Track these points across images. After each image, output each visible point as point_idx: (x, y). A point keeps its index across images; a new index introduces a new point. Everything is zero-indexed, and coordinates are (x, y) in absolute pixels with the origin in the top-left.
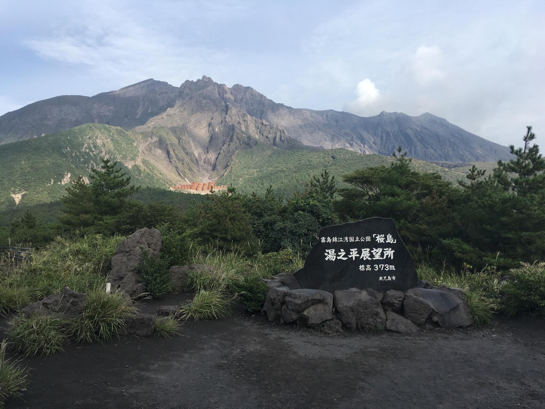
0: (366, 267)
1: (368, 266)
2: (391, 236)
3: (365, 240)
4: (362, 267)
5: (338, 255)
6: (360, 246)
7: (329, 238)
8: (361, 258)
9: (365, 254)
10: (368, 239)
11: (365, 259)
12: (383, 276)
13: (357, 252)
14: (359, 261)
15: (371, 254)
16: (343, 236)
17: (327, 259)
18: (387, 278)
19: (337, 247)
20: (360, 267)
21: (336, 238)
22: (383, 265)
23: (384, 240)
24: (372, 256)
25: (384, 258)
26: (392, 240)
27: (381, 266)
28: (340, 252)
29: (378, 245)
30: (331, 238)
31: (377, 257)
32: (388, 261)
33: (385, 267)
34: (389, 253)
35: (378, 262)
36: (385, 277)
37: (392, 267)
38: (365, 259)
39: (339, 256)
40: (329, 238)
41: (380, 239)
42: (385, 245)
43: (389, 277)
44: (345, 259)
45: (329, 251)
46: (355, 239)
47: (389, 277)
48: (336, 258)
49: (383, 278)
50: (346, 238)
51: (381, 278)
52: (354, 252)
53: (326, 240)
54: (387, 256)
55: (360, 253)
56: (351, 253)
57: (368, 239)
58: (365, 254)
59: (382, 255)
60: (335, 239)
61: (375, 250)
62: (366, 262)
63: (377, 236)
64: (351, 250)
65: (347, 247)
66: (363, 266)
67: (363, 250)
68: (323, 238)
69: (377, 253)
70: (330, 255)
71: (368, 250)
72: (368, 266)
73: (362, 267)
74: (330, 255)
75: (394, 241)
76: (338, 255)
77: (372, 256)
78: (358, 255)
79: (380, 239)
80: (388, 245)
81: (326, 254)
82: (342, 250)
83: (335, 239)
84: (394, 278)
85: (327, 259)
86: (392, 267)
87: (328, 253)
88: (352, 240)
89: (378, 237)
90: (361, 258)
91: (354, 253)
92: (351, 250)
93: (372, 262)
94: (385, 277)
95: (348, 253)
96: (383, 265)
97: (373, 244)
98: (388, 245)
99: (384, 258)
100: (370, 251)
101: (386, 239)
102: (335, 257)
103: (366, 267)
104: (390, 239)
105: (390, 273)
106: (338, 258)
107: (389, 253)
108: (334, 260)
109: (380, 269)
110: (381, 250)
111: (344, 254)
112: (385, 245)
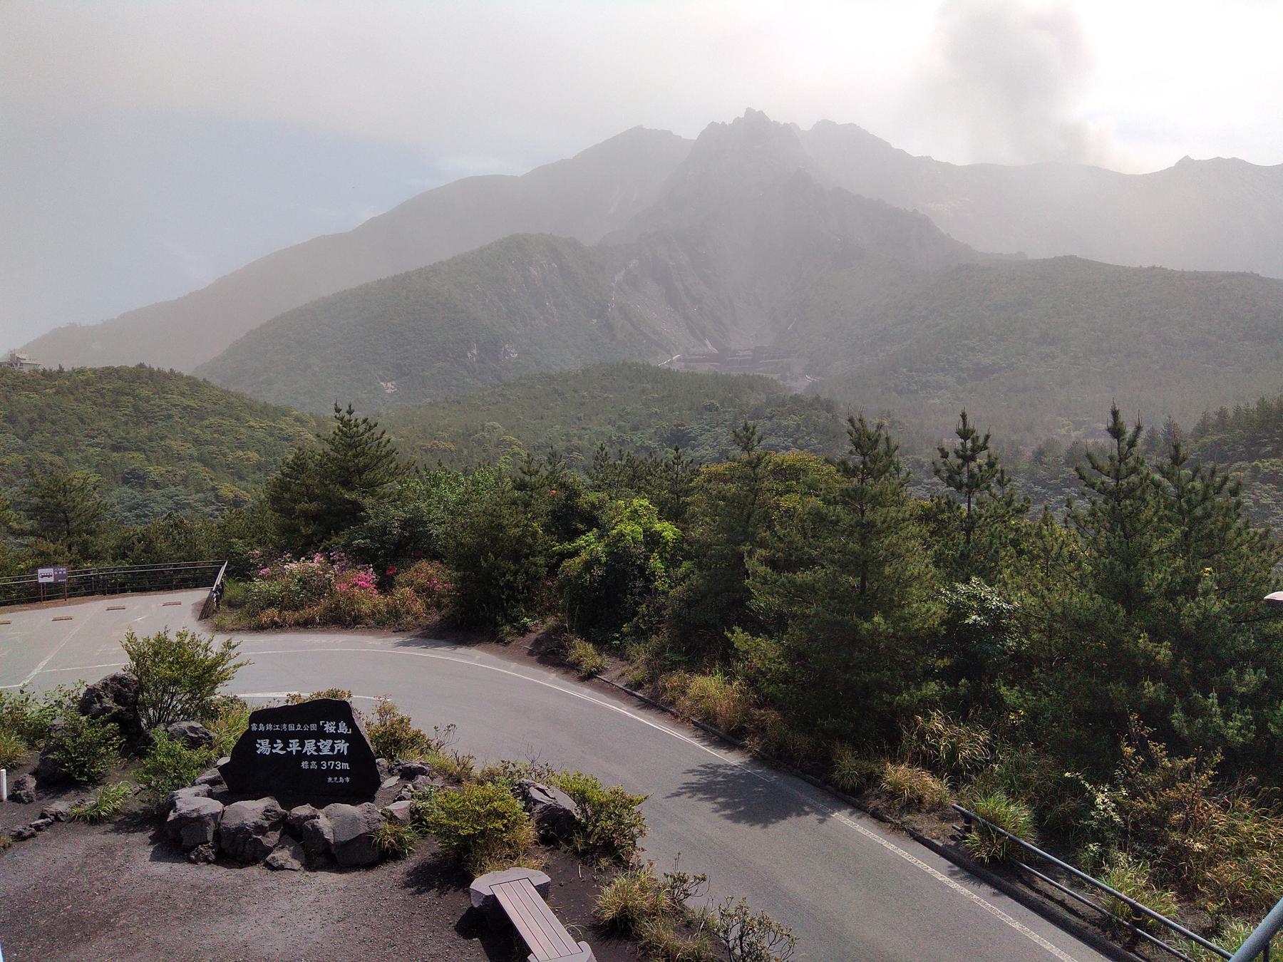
1: (314, 763)
4: (304, 765)
5: (273, 748)
6: (302, 737)
9: (310, 747)
10: (314, 727)
14: (301, 756)
16: (280, 723)
19: (272, 737)
24: (318, 750)
31: (326, 751)
32: (340, 757)
34: (342, 746)
35: (327, 758)
37: (346, 766)
41: (329, 727)
42: (336, 736)
45: (262, 741)
55: (302, 745)
57: (314, 727)
58: (310, 747)
59: (332, 749)
60: (269, 727)
62: (312, 758)
69: (325, 747)
70: (264, 747)
72: (314, 763)
74: (264, 747)
76: (273, 748)
77: (318, 750)
79: (329, 727)
83: (269, 727)
84: (348, 779)
86: (346, 766)
88: (291, 727)
91: (294, 746)
93: (319, 759)
95: (286, 745)
97: (320, 735)
104: (343, 728)
105: (343, 773)
107: (342, 746)
109: (329, 767)
112: (336, 736)
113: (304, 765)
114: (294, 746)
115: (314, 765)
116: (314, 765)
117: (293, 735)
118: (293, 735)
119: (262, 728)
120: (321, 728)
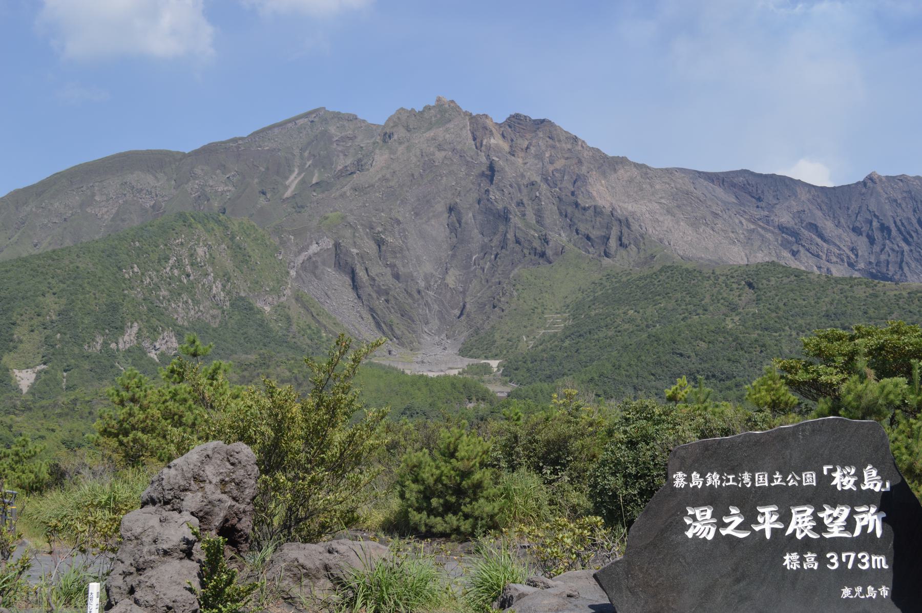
0: (802, 560)
1: (810, 557)
2: (874, 473)
3: (800, 482)
6: (785, 500)
7: (695, 475)
8: (789, 531)
9: (801, 522)
10: (809, 479)
11: (799, 536)
12: (853, 586)
13: (775, 517)
14: (783, 542)
15: (819, 521)
16: (736, 470)
17: (689, 534)
18: (865, 592)
19: (719, 501)
20: (787, 557)
21: (716, 476)
22: (853, 555)
23: (856, 484)
24: (820, 527)
25: (857, 532)
26: (879, 485)
27: (848, 558)
28: (728, 514)
29: (837, 498)
30: (703, 475)
31: (836, 531)
32: (867, 542)
33: (857, 561)
34: (871, 519)
35: (839, 545)
36: (859, 589)
38: (799, 536)
39: (726, 525)
40: (695, 475)
41: (843, 480)
42: (856, 498)
43: (870, 588)
44: (742, 535)
45: (698, 512)
46: (771, 480)
47: (870, 588)
48: (717, 533)
49: (853, 593)
50: (746, 477)
51: (846, 592)
52: (767, 516)
53: (688, 479)
54: (865, 528)
55: (785, 518)
56: (760, 519)
57: (809, 479)
58: (801, 522)
59: (850, 524)
60: (713, 479)
61: (828, 511)
62: (805, 546)
63: (835, 470)
64: (761, 510)
65: (749, 502)
66: (795, 556)
67: (794, 510)
68: (680, 474)
69: (836, 520)
70: (701, 524)
71: (810, 510)
72: (810, 557)
73: (791, 561)
74: (701, 524)
75: (884, 486)
77: (820, 527)
78: (779, 526)
79: (843, 480)
80: (866, 498)
81: (688, 521)
82: (734, 510)
83: (713, 479)
85: (689, 534)
86: (880, 562)
87: (694, 518)
88: (762, 480)
89: (837, 475)
90: (789, 531)
91: (768, 520)
92: (761, 510)
93: (820, 545)
94: (859, 589)
95: (750, 518)
96: (853, 555)
97: (825, 495)
98: (866, 498)
99: (857, 532)
100: (815, 516)
101: (860, 480)
102: (713, 530)
103: (802, 560)
104: (873, 481)
105: (874, 577)
106: (724, 532)
108: (710, 537)
109: (843, 565)
110: (846, 511)
111: (738, 520)
112: (856, 498)
113: (791, 561)
114: (768, 520)
115: (811, 561)
116: (811, 561)
117: (766, 496)
118: (766, 496)
119: (696, 480)
120: (825, 481)
